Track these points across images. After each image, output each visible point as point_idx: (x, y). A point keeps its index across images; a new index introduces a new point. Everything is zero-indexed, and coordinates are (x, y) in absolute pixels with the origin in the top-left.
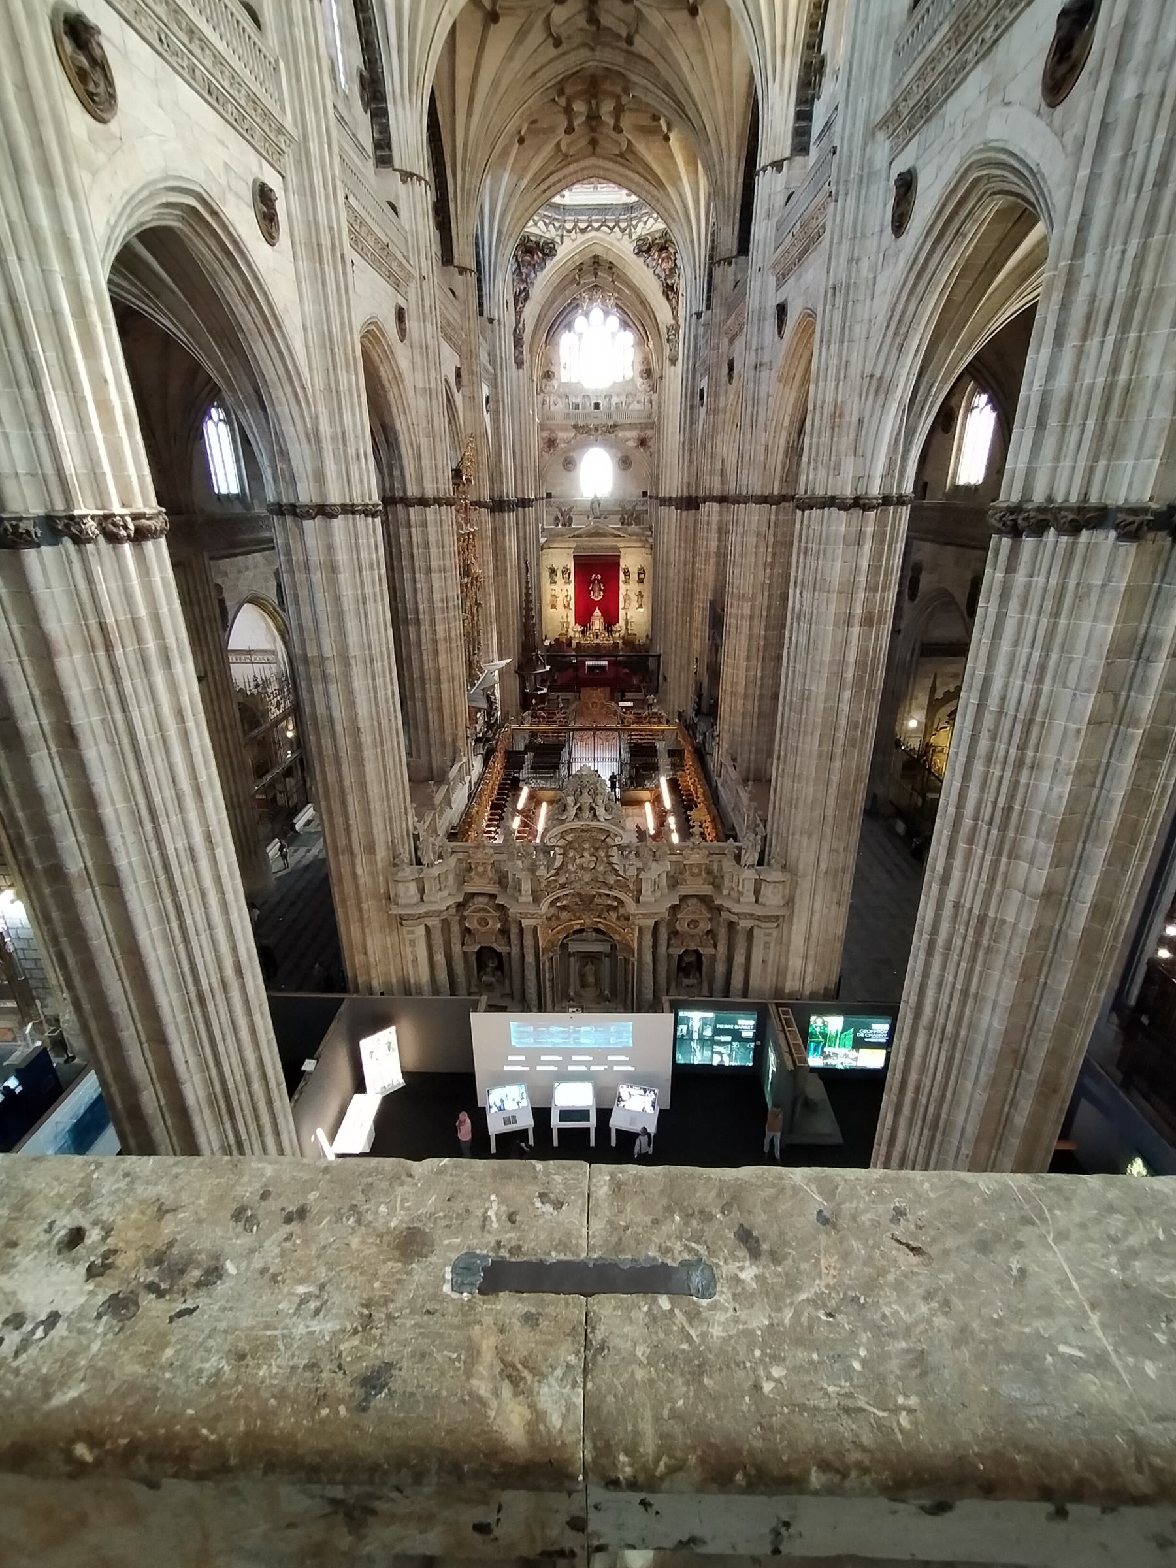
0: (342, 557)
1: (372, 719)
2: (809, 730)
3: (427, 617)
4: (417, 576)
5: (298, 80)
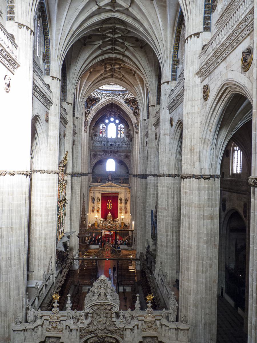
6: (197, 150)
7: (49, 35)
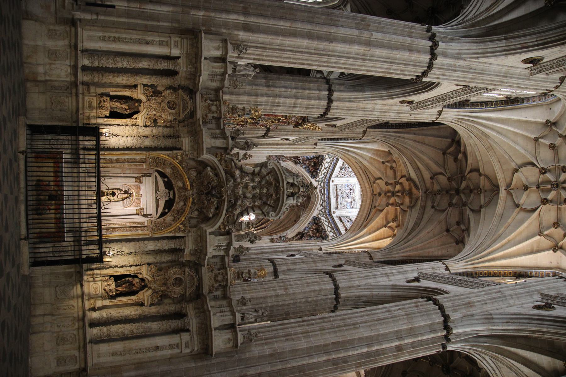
0: (415, 57)
1: (333, 51)
2: (338, 334)
3: (270, 92)
4: (295, 90)
5: (540, 81)
6: (475, 311)
7: (486, 108)
